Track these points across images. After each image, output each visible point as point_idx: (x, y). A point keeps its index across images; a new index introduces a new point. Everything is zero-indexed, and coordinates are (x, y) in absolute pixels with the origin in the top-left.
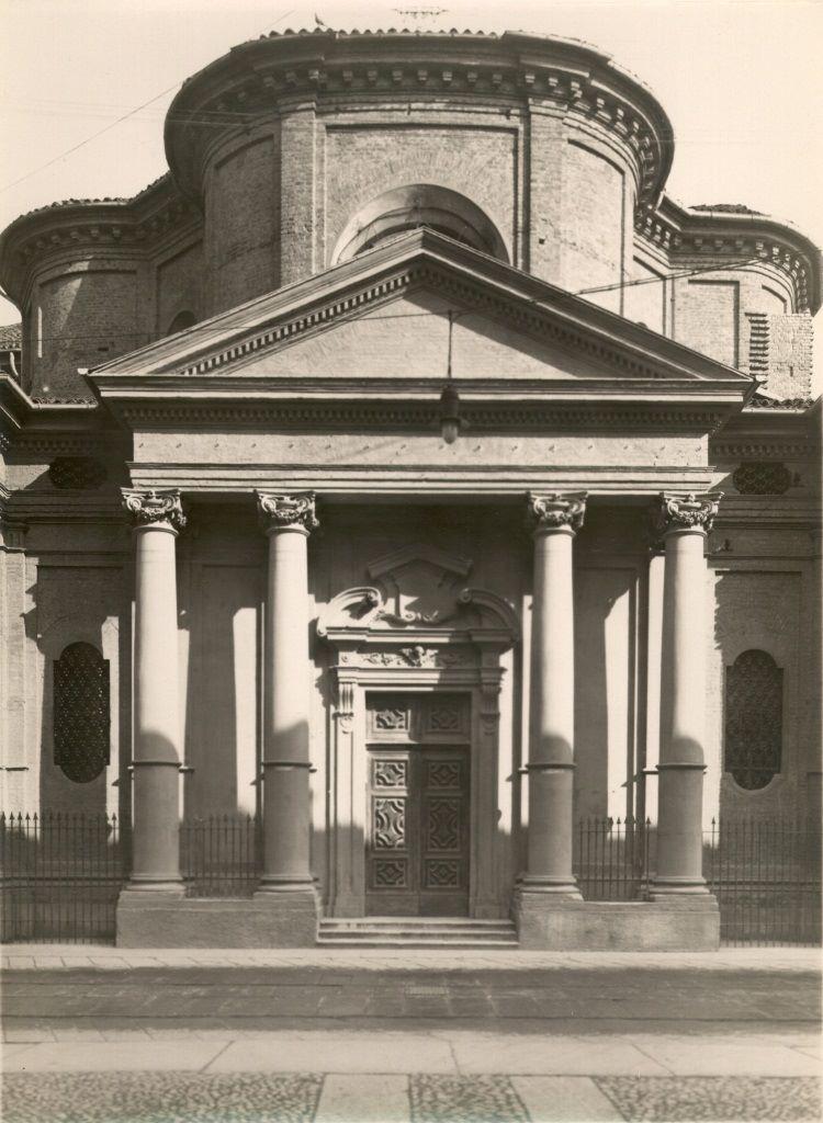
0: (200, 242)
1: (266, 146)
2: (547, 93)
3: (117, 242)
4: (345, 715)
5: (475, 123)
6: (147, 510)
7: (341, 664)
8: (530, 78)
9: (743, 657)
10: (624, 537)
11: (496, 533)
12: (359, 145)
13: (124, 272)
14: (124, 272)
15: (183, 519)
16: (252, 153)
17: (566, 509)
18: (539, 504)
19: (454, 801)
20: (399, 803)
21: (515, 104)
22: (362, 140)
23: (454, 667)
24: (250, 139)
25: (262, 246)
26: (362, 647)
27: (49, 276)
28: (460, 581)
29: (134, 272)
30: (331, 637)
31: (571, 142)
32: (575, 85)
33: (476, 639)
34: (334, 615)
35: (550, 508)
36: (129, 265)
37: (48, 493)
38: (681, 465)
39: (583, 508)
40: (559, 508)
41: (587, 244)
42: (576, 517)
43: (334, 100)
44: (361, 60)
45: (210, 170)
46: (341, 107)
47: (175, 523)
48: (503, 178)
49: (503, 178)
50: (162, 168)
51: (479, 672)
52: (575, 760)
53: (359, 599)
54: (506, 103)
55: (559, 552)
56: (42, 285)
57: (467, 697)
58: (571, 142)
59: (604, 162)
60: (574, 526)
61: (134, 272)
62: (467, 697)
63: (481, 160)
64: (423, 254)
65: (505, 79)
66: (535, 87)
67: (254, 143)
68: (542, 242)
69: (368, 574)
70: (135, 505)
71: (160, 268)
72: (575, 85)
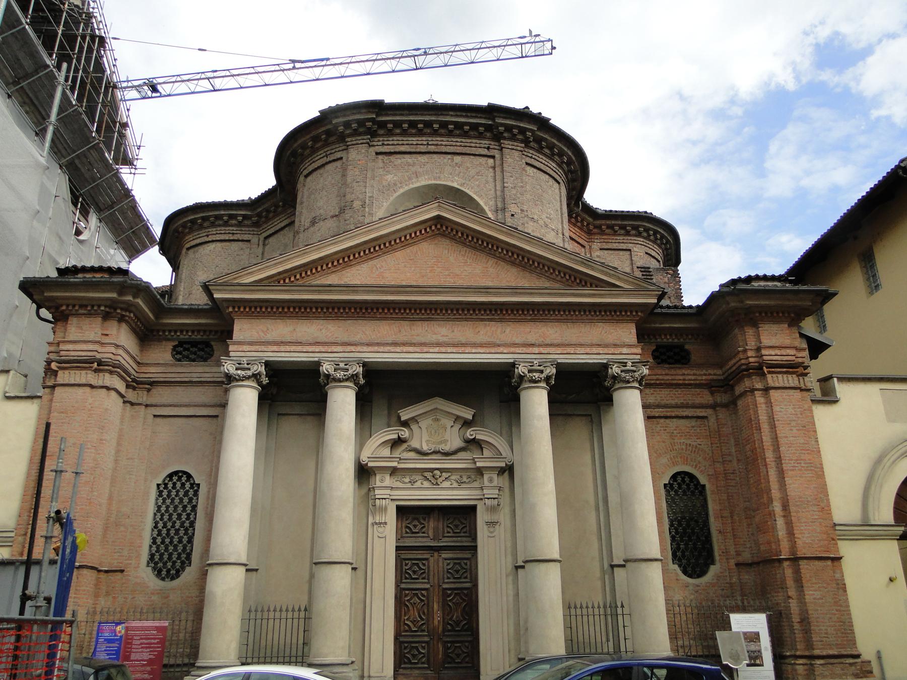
0: (293, 223)
1: (338, 163)
2: (513, 138)
3: (240, 224)
4: (380, 523)
5: (468, 152)
6: (239, 372)
7: (378, 484)
8: (501, 129)
9: (674, 477)
10: (582, 394)
11: (490, 391)
12: (396, 163)
13: (243, 241)
14: (243, 241)
15: (265, 381)
16: (328, 167)
17: (542, 372)
18: (521, 369)
19: (466, 592)
20: (423, 596)
21: (493, 143)
22: (398, 160)
23: (463, 486)
24: (329, 159)
25: (332, 217)
26: (394, 471)
27: (193, 243)
28: (467, 424)
29: (249, 241)
30: (370, 464)
31: (527, 164)
32: (529, 134)
33: (479, 464)
34: (375, 449)
35: (530, 371)
36: (246, 237)
37: (172, 365)
38: (612, 345)
39: (554, 371)
40: (536, 371)
41: (541, 215)
42: (547, 379)
43: (381, 139)
44: (398, 118)
45: (302, 178)
46: (386, 143)
47: (260, 383)
48: (487, 182)
49: (487, 182)
50: (270, 181)
51: (482, 489)
52: (561, 556)
53: (395, 436)
54: (487, 142)
55: (536, 403)
56: (188, 249)
57: (473, 508)
58: (527, 164)
59: (547, 176)
60: (548, 384)
61: (249, 241)
62: (473, 508)
63: (473, 172)
64: (439, 217)
65: (486, 130)
66: (506, 135)
67: (330, 162)
68: (513, 215)
69: (399, 417)
70: (231, 369)
71: (266, 238)
72: (529, 134)
